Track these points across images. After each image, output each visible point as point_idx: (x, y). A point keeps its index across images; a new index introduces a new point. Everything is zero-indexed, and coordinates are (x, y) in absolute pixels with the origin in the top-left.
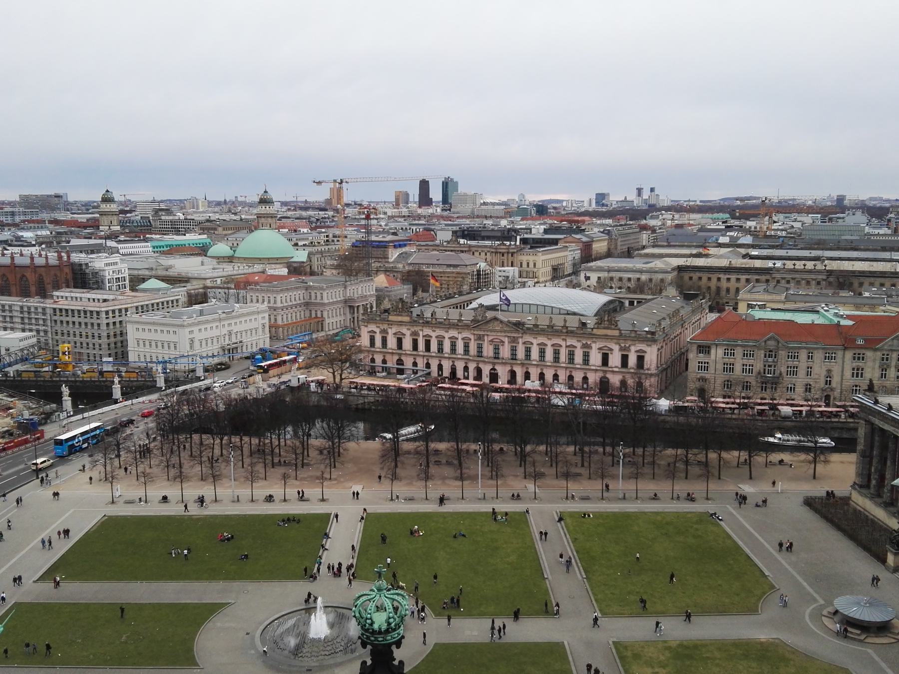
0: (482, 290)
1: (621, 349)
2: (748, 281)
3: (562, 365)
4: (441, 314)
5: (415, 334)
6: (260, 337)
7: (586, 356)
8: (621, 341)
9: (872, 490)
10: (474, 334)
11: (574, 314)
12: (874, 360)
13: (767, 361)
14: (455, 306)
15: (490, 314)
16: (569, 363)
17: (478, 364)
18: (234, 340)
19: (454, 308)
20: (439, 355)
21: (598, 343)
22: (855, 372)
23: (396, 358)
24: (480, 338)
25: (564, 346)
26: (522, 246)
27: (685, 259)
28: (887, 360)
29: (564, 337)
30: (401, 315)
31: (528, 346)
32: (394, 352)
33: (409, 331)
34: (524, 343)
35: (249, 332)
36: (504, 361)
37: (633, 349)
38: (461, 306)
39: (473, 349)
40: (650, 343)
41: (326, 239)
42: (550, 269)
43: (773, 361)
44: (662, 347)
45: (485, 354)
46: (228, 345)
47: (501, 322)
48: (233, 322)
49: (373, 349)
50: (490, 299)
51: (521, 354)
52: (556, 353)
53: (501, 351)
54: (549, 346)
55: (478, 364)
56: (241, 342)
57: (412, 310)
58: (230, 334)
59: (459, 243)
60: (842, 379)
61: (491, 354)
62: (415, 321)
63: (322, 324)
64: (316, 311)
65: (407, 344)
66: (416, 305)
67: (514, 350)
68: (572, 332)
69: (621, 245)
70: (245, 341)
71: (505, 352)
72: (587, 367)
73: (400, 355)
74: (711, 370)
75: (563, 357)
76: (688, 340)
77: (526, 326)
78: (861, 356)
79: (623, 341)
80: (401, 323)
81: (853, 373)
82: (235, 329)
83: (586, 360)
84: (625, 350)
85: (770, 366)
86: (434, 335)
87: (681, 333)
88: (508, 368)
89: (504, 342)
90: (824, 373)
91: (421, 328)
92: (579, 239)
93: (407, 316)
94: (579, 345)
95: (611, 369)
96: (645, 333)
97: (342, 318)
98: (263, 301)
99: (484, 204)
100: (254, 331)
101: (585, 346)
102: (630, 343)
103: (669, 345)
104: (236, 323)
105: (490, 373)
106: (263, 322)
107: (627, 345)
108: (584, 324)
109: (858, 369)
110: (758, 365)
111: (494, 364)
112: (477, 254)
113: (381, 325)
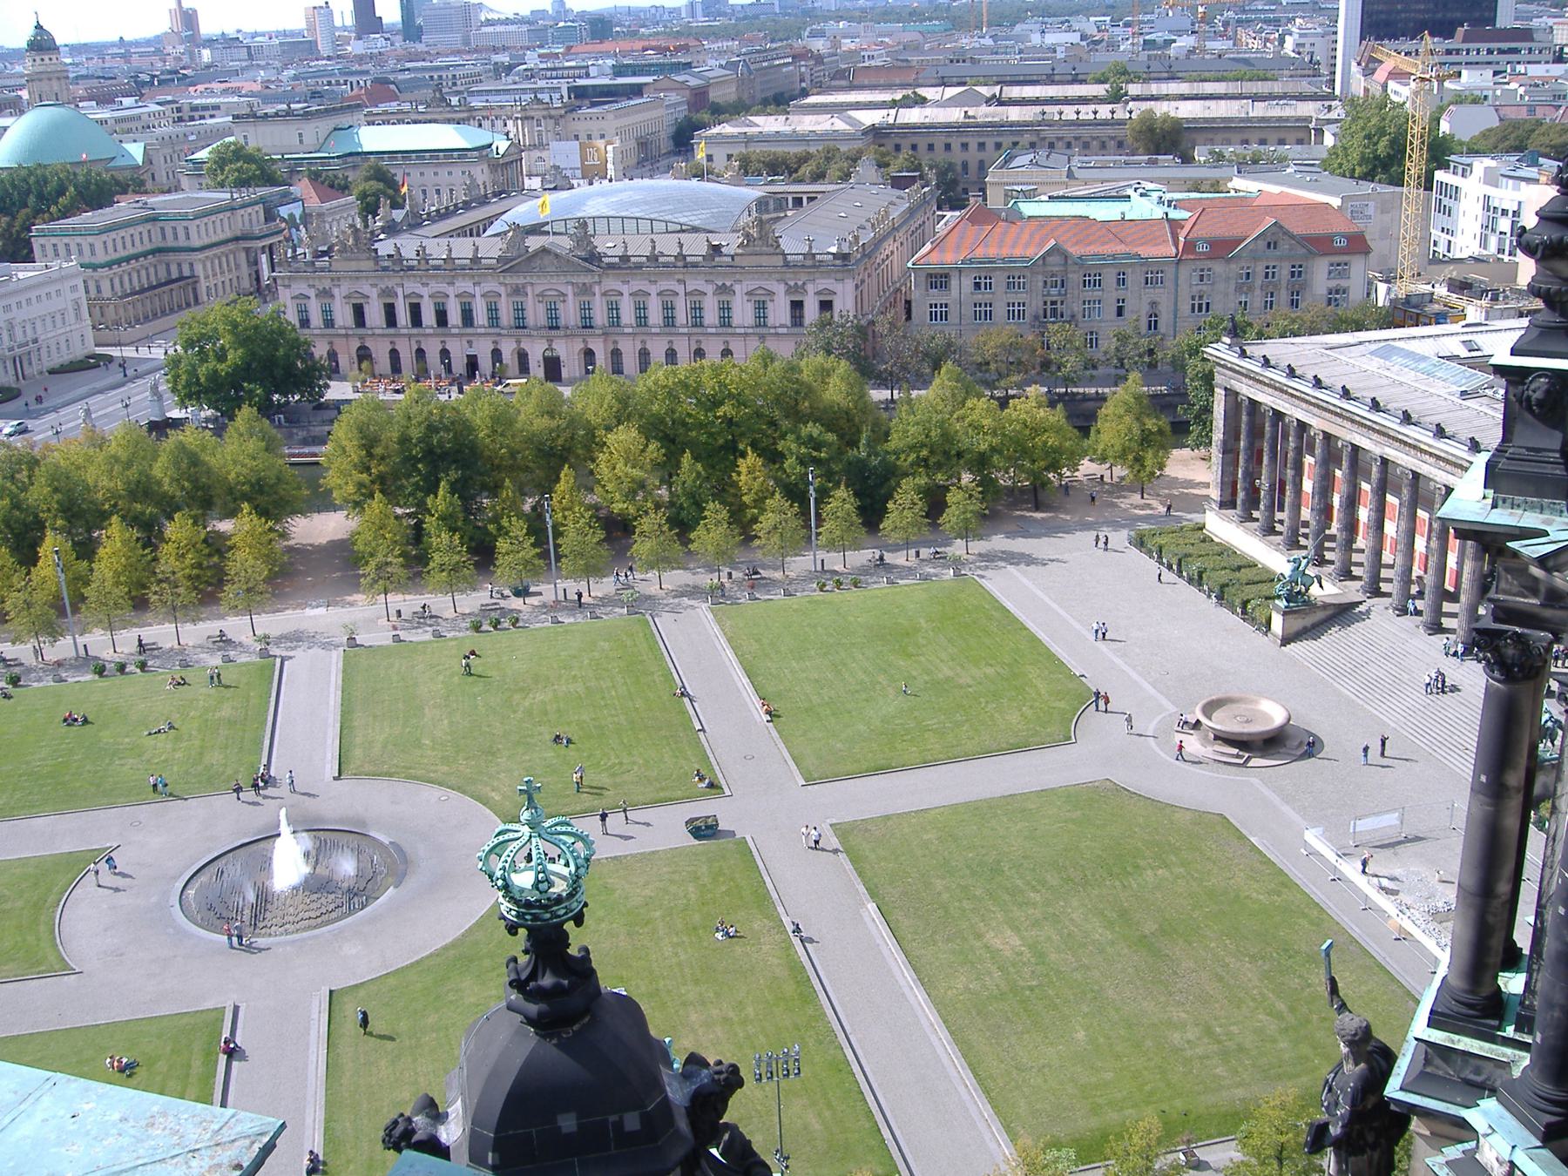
0: (509, 196)
1: (789, 291)
2: (998, 146)
3: (681, 330)
4: (437, 250)
5: (388, 292)
6: (73, 327)
7: (725, 309)
8: (788, 276)
9: (1239, 511)
10: (506, 285)
11: (695, 230)
12: (1228, 279)
13: (1049, 295)
14: (468, 229)
15: (534, 243)
16: (695, 325)
17: (518, 342)
18: (20, 338)
19: (459, 235)
20: (441, 330)
21: (745, 283)
22: (1196, 302)
23: (356, 344)
24: (517, 291)
25: (682, 293)
26: (578, 103)
27: (884, 112)
28: (1248, 278)
29: (681, 277)
30: (358, 260)
31: (613, 298)
32: (350, 332)
33: (374, 290)
34: (604, 294)
35: (49, 320)
36: (569, 332)
37: (810, 288)
38: (471, 230)
39: (506, 316)
40: (839, 276)
41: (176, 115)
42: (633, 144)
43: (1060, 294)
44: (863, 281)
45: (530, 321)
46: (11, 349)
47: (557, 256)
48: (13, 301)
49: (306, 331)
50: (522, 212)
51: (600, 316)
52: (669, 309)
53: (561, 313)
54: (654, 295)
55: (518, 342)
56: (35, 341)
57: (377, 245)
58: (11, 327)
59: (449, 105)
60: (1176, 317)
61: (543, 320)
62: (385, 269)
63: (195, 290)
64: (179, 265)
65: (375, 315)
66: (382, 236)
67: (586, 309)
68: (695, 265)
69: (762, 91)
70: (43, 337)
71: (569, 313)
72: (730, 330)
73: (362, 337)
74: (953, 317)
75: (681, 316)
76: (910, 265)
77: (606, 260)
78: (1205, 273)
79: (792, 276)
80: (357, 276)
81: (1193, 305)
82: (19, 315)
83: (725, 321)
84: (796, 291)
85: (1053, 303)
86: (425, 292)
87: (892, 252)
88: (579, 345)
89: (564, 295)
90: (1145, 309)
91: (398, 280)
92: (683, 83)
93: (368, 259)
94: (709, 289)
95: (772, 331)
96: (831, 257)
97: (233, 275)
98: (69, 253)
99: (489, 23)
100: (58, 317)
101: (723, 290)
102: (804, 278)
103: (874, 274)
104: (19, 304)
105: (545, 359)
106: (75, 295)
107: (800, 283)
108: (716, 249)
109: (1201, 298)
110: (1034, 303)
111: (550, 341)
112: (486, 123)
113: (317, 283)
